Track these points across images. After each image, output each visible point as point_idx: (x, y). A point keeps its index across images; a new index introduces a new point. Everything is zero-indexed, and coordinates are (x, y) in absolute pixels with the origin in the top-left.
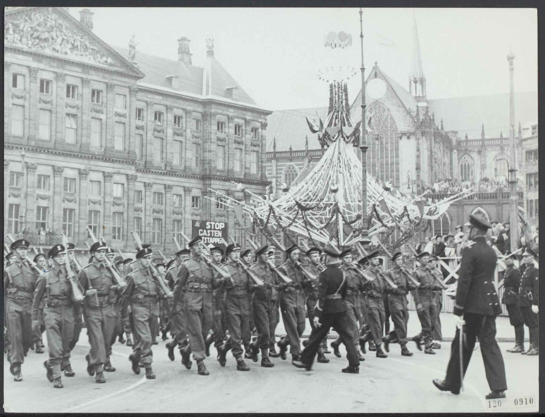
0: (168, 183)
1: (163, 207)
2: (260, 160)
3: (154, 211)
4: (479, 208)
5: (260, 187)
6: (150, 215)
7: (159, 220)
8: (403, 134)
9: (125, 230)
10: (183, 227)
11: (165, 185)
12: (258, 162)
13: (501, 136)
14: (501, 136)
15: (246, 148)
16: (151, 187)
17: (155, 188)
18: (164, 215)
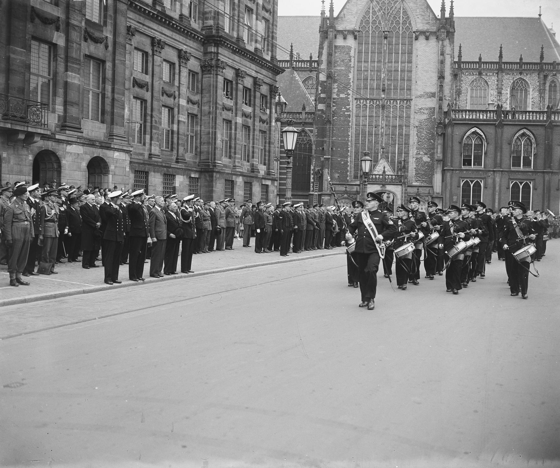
0: (158, 36)
1: (147, 79)
2: (270, 35)
3: (137, 83)
4: (525, 130)
5: (270, 75)
6: (129, 89)
7: (143, 101)
8: (423, 33)
9: (108, 101)
10: (176, 119)
11: (153, 39)
12: (268, 36)
13: (480, 59)
14: (480, 59)
15: (257, 9)
16: (133, 35)
17: (137, 39)
18: (149, 93)
